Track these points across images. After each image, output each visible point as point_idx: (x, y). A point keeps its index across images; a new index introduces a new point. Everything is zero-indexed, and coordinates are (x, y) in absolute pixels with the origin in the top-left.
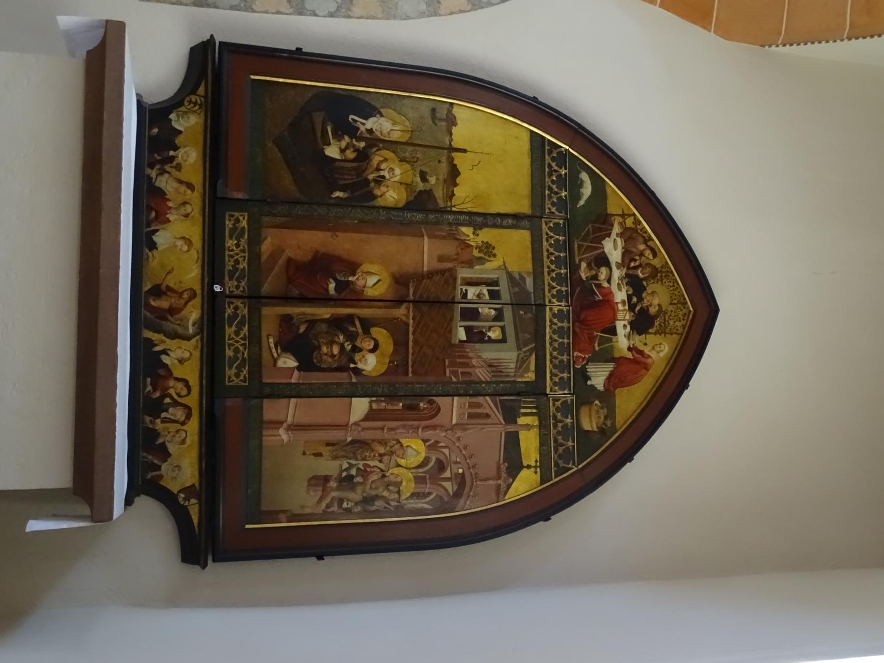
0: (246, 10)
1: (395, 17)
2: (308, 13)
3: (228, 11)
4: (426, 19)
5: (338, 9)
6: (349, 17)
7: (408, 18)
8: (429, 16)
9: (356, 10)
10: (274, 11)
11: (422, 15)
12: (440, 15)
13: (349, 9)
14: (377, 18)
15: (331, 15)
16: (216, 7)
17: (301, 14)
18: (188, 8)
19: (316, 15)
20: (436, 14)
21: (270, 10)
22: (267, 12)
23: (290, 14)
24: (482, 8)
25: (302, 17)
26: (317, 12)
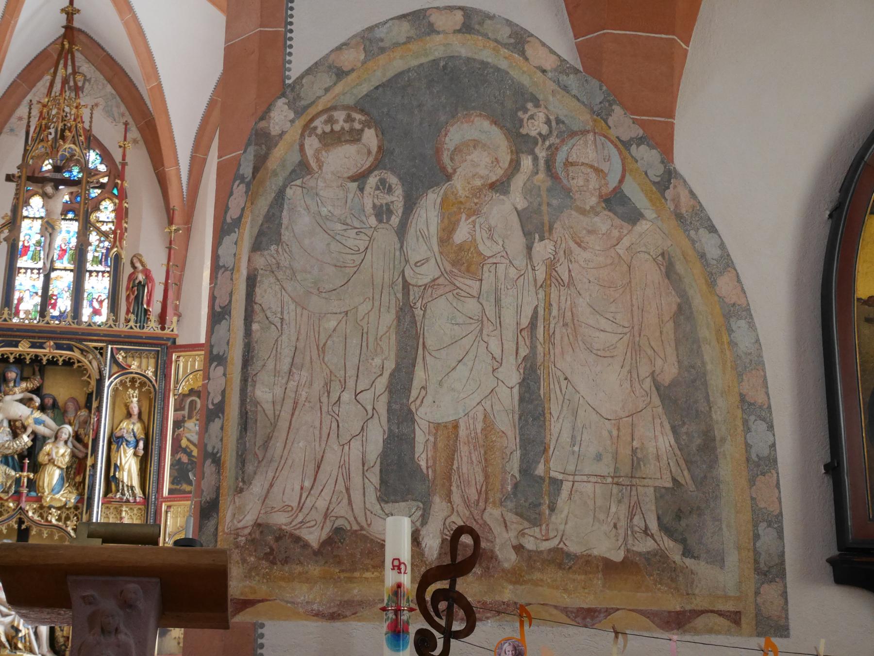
0: (781, 522)
1: (760, 356)
2: (773, 453)
3: (785, 541)
4: (756, 320)
5: (764, 420)
6: (769, 407)
7: (757, 341)
8: (752, 318)
9: (760, 399)
10: (777, 491)
11: (752, 326)
12: (748, 304)
13: (760, 407)
14: (765, 376)
15: (771, 427)
16: (783, 553)
17: (775, 461)
18: (788, 585)
19: (773, 445)
20: (748, 310)
21: (777, 495)
22: (779, 499)
23: (778, 474)
24: (728, 255)
25: (779, 460)
26: (770, 443)
